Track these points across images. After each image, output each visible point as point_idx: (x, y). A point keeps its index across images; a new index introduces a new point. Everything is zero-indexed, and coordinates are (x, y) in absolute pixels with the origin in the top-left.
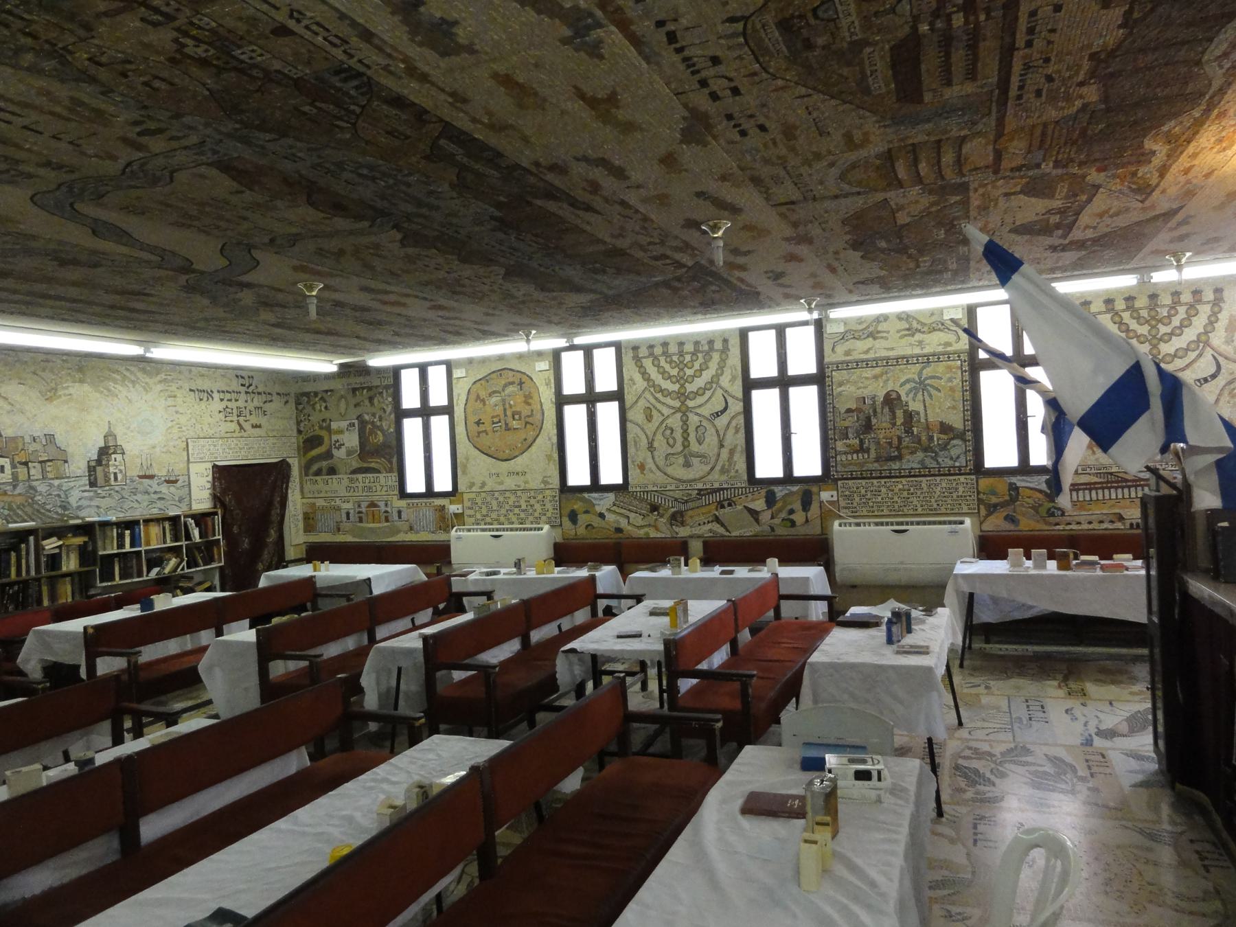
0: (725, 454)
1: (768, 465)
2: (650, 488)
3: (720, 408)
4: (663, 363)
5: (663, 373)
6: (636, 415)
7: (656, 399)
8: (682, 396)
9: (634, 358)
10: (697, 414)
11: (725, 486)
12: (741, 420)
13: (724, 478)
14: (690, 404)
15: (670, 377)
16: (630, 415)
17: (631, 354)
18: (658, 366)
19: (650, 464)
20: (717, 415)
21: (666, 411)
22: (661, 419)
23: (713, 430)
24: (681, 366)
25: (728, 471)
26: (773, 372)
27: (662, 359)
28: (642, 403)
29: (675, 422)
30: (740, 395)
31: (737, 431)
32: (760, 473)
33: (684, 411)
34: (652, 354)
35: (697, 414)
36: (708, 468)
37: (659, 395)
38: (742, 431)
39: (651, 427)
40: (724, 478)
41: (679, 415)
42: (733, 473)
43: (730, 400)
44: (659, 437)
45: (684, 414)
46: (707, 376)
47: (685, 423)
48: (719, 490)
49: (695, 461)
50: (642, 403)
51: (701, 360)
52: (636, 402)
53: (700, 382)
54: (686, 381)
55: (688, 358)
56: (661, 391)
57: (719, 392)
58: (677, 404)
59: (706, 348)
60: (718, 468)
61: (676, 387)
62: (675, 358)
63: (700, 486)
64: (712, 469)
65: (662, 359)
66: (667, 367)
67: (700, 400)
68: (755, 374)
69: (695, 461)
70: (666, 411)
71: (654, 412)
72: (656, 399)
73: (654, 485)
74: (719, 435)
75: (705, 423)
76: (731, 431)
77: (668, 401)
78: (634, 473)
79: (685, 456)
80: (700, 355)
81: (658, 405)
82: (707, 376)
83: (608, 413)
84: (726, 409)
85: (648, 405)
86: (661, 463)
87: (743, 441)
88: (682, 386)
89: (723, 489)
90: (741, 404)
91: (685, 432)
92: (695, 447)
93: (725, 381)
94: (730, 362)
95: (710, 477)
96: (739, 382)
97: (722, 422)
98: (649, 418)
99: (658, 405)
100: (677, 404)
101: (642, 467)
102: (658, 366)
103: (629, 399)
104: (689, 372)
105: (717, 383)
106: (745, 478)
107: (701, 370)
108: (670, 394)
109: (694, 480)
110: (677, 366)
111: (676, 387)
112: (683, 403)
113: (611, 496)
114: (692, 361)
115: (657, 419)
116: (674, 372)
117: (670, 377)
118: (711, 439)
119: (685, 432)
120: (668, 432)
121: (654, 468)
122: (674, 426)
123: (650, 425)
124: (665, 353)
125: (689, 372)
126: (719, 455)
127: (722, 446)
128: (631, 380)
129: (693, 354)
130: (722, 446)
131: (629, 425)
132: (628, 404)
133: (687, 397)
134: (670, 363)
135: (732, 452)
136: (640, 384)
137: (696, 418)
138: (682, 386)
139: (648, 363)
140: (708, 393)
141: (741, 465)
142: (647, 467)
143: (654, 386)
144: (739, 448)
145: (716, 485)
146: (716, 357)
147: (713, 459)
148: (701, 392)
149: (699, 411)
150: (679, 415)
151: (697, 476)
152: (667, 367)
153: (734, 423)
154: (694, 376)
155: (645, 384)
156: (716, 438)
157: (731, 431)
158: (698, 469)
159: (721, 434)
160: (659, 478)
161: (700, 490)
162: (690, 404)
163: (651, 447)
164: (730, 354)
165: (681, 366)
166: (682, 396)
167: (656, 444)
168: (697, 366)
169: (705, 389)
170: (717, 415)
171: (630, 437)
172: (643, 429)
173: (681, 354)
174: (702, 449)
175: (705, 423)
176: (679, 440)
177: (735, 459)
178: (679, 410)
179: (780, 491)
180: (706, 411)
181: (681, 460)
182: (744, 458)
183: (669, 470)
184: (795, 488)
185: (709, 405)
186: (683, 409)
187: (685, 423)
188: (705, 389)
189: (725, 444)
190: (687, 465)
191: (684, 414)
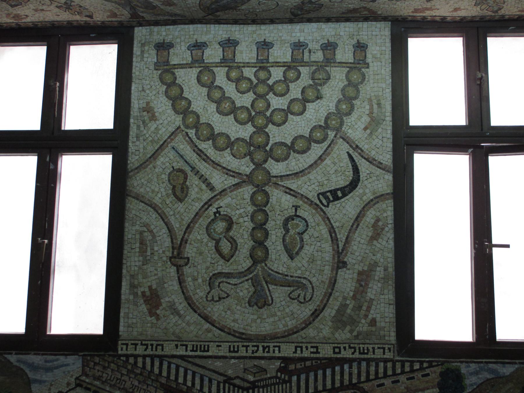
0: (347, 282)
1: (442, 314)
2: (169, 349)
3: (341, 181)
4: (221, 79)
5: (221, 101)
6: (153, 183)
7: (200, 153)
8: (259, 149)
9: (157, 66)
10: (289, 191)
11: (347, 354)
12: (387, 210)
13: (344, 335)
14: (276, 168)
15: (234, 110)
16: (137, 183)
17: (151, 57)
18: (211, 86)
19: (172, 294)
20: (335, 195)
21: (219, 180)
22: (207, 195)
23: (324, 231)
24: (262, 88)
25: (353, 322)
26: (456, 115)
27: (221, 74)
28: (166, 160)
29: (238, 204)
30: (387, 158)
31: (376, 236)
32: (425, 330)
33: (260, 184)
34: (197, 62)
35: (289, 191)
36: (306, 311)
37: (206, 146)
38: (389, 235)
39: (181, 213)
40: (344, 335)
41: (247, 191)
42: (363, 326)
43: (364, 167)
44: (198, 234)
45: (260, 189)
46: (315, 113)
47: (261, 208)
48: (331, 363)
49: (279, 294)
50: (166, 160)
51: (305, 80)
52: (155, 156)
53: (299, 126)
54: (270, 120)
55: (277, 74)
56: (213, 137)
57: (341, 149)
58: (245, 166)
59: (319, 56)
60: (329, 312)
61: (246, 131)
62: (249, 73)
63: (288, 351)
64: (316, 314)
65: (221, 74)
66: (230, 89)
67: (297, 162)
68: (420, 116)
69: (279, 294)
70: (219, 180)
71: (193, 181)
72: (200, 153)
73: (180, 342)
74: (334, 240)
75: (306, 212)
76: (363, 234)
77: (226, 159)
78: (133, 314)
79: (255, 282)
80: (304, 71)
81: (203, 168)
82: (315, 113)
83: (87, 179)
84: (354, 184)
85: (179, 164)
86: (199, 294)
87: (390, 256)
88: (260, 130)
89: (342, 361)
90: (389, 177)
91: (260, 227)
92: (278, 261)
93: (355, 126)
94: (368, 90)
95: (311, 332)
96: (386, 131)
97: (345, 210)
98: (180, 192)
99: (203, 168)
100: (245, 166)
101: (153, 300)
102: (211, 86)
103: (137, 149)
104: (277, 102)
105: (338, 130)
106: (392, 338)
107: (305, 101)
108: (230, 144)
109: (274, 337)
110: (252, 88)
111: (246, 131)
112: (258, 166)
113: (73, 364)
114: (286, 80)
115: (197, 193)
116: (245, 100)
117: (234, 110)
118: (317, 248)
119: (260, 227)
120: (221, 226)
121: (182, 306)
122: (235, 215)
123: (180, 207)
124: (227, 62)
125: (277, 102)
126: (333, 283)
127: (340, 264)
128: (148, 109)
129: (288, 67)
130: (340, 264)
131: (133, 207)
132: (133, 160)
133: (270, 155)
134: (237, 81)
135: (364, 278)
136: (167, 118)
137: (287, 201)
138: (260, 130)
139: (188, 78)
140: (317, 150)
141: (384, 311)
142: (165, 301)
143: (197, 125)
144: (379, 272)
145: (326, 351)
146: (338, 77)
147: (319, 295)
148: (300, 145)
149: (288, 183)
150: (247, 191)
151: (281, 328)
152: (230, 89)
153: (370, 216)
154: (288, 111)
155: (178, 120)
156: (327, 246)
157: (363, 234)
158: (284, 312)
159: (342, 237)
160: (192, 326)
161: (285, 360)
162: (276, 168)
163: (178, 257)
164: (369, 72)
165: (262, 88)
166: (259, 149)
167: (190, 251)
168: (295, 91)
169: (310, 140)
170: (335, 195)
171: (131, 231)
172: (163, 217)
173: (263, 65)
174: (298, 267)
175: (306, 212)
176: (245, 244)
177: (370, 294)
178: (249, 179)
179: (472, 374)
180: (309, 186)
181: (246, 290)
182: (390, 296)
183: (216, 311)
184: (507, 370)
185: (315, 175)
186: (260, 177)
187: (261, 208)
188: (310, 140)
189: (349, 259)
190: (259, 301)
191: (260, 189)
